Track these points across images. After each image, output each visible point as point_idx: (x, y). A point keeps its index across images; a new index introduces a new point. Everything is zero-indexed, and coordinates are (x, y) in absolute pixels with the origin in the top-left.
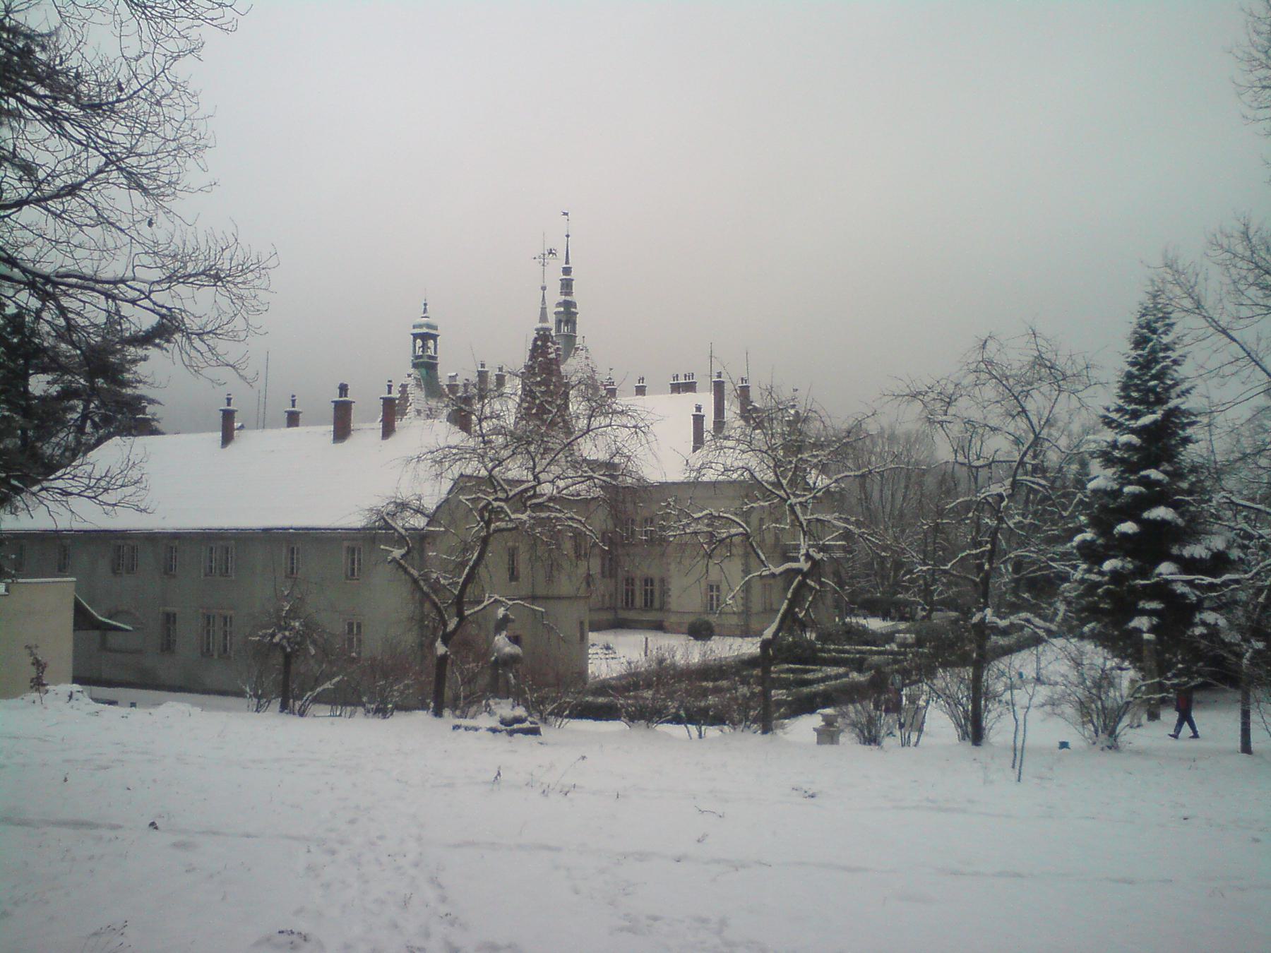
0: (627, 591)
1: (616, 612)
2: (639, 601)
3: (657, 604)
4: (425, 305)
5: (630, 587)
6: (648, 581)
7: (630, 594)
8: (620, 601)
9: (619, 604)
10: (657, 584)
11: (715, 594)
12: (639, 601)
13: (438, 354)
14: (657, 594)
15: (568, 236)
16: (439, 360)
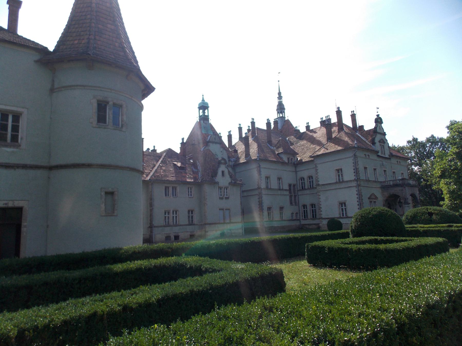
0: (304, 211)
1: (300, 221)
2: (310, 216)
3: (318, 217)
4: (203, 96)
5: (305, 209)
6: (313, 205)
7: (305, 213)
8: (301, 216)
9: (301, 218)
10: (317, 207)
11: (344, 207)
12: (310, 216)
13: (209, 115)
14: (317, 211)
15: (279, 81)
16: (210, 117)
